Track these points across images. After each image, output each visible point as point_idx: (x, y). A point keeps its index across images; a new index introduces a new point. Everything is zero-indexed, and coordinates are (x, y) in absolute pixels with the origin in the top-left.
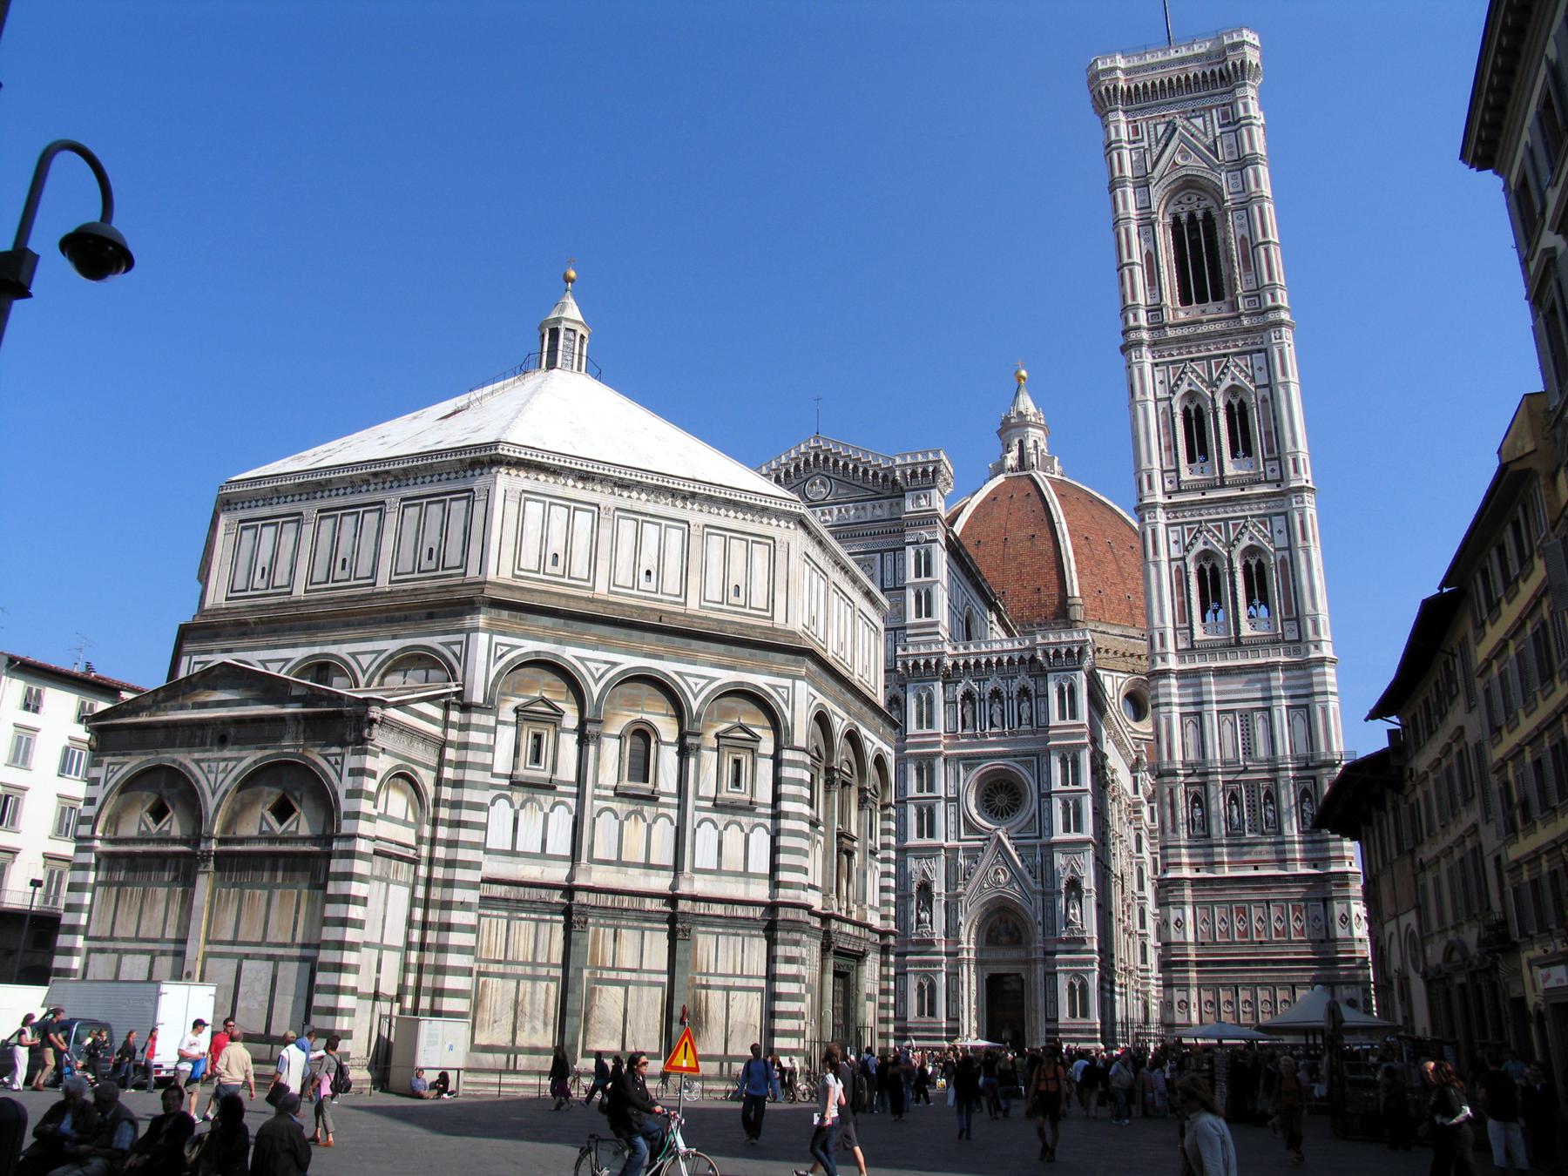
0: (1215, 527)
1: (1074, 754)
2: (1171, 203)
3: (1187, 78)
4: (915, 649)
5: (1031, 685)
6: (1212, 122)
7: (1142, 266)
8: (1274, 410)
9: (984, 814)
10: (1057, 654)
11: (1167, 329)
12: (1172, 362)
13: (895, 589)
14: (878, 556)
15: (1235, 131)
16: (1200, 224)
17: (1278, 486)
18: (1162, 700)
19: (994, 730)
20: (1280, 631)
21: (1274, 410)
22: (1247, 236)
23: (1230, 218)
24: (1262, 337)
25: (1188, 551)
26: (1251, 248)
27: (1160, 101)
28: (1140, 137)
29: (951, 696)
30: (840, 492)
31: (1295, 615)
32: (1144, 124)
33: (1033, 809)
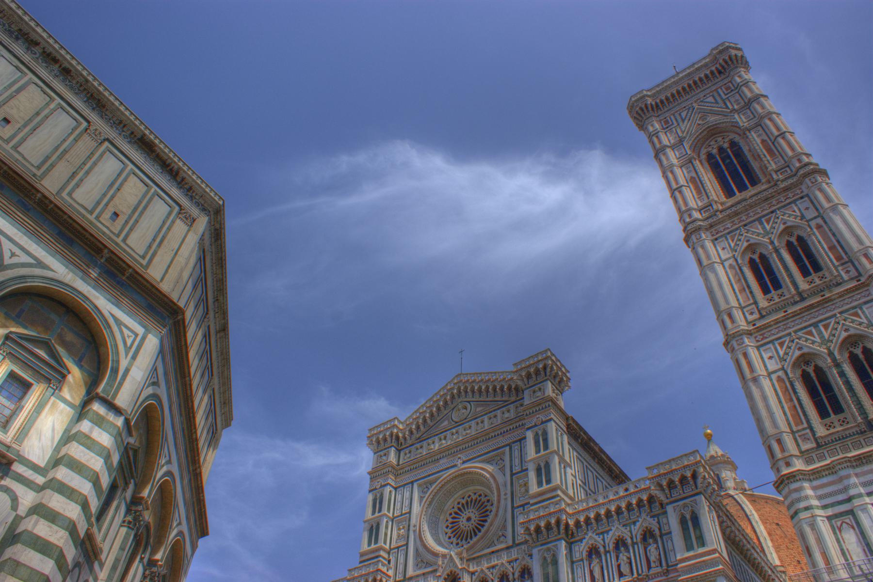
0: (806, 333)
2: (703, 147)
4: (536, 515)
5: (653, 524)
6: (719, 95)
7: (689, 187)
8: (831, 230)
10: (671, 483)
12: (729, 233)
13: (522, 471)
14: (507, 448)
15: (738, 92)
16: (729, 150)
17: (858, 281)
21: (831, 230)
22: (766, 138)
23: (748, 134)
24: (800, 189)
28: (671, 123)
29: (578, 555)
32: (672, 117)
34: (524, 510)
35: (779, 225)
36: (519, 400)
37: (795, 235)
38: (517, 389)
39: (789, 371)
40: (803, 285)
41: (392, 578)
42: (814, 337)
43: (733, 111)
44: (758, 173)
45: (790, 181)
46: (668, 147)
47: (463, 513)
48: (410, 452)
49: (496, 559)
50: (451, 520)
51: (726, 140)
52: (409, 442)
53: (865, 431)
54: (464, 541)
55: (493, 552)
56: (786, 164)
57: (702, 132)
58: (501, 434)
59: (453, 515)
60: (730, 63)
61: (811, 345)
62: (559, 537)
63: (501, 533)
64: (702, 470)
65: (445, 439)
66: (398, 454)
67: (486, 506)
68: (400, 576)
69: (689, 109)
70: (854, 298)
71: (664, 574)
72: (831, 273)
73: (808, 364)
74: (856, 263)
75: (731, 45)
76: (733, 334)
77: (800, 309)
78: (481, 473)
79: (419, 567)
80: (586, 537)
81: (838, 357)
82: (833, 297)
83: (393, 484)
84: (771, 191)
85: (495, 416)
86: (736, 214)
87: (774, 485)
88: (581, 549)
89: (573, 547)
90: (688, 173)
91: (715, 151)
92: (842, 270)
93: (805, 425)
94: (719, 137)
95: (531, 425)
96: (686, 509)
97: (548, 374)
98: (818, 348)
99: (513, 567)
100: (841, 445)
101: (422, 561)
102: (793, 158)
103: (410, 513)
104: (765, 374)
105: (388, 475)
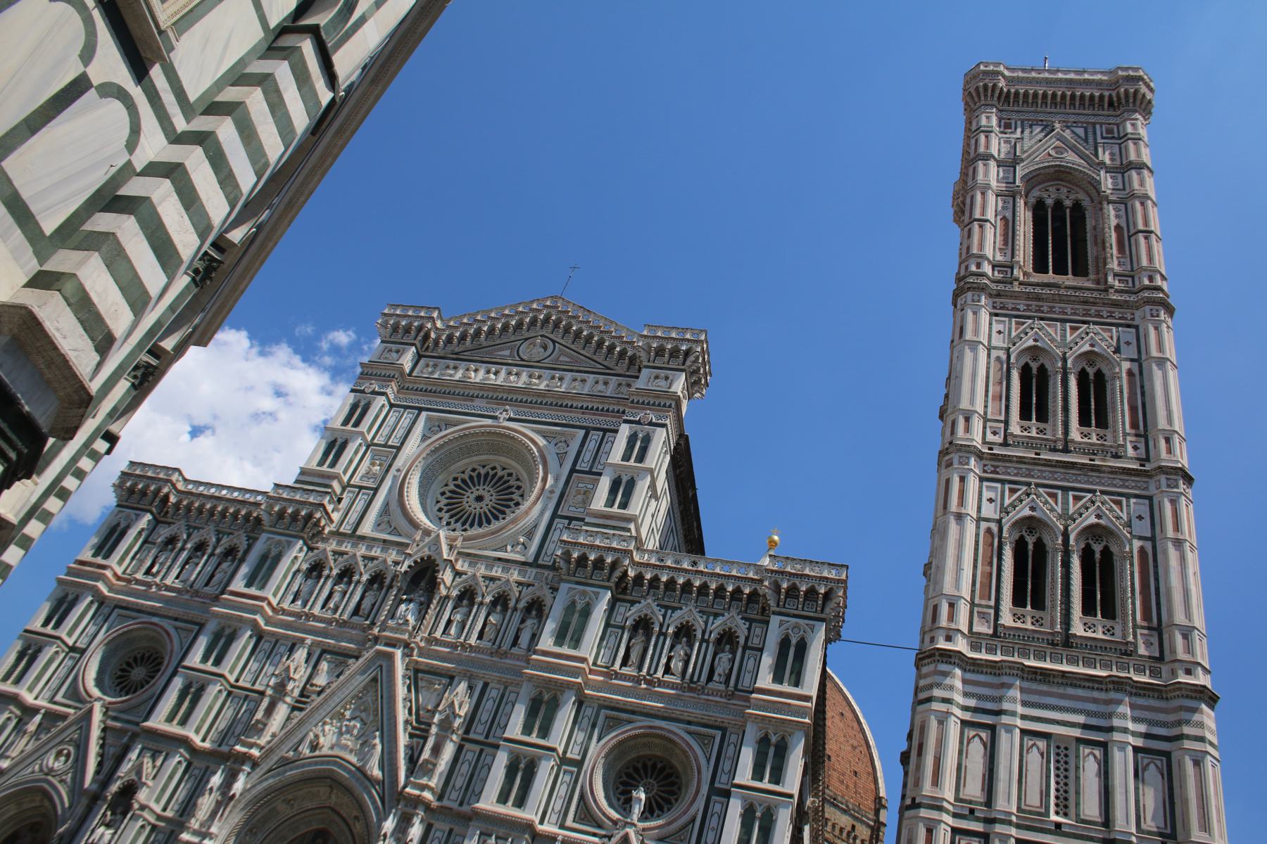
0: (1051, 495)
1: (783, 738)
2: (1038, 188)
3: (1073, 96)
5: (741, 629)
6: (1095, 133)
7: (995, 227)
8: (1142, 387)
9: (614, 801)
11: (1016, 283)
13: (590, 472)
14: (582, 432)
15: (1120, 144)
16: (1068, 211)
18: (937, 693)
19: (668, 678)
20: (1131, 638)
21: (1142, 387)
22: (1124, 225)
24: (1133, 314)
25: (1008, 513)
26: (1127, 235)
27: (1039, 109)
29: (619, 619)
30: (562, 358)
31: (1158, 627)
32: (1019, 123)
33: (692, 811)
34: (569, 524)
35: (1085, 343)
36: (628, 376)
37: (1096, 368)
38: (633, 360)
39: (1005, 529)
40: (1075, 435)
41: (334, 525)
42: (1056, 504)
43: (1102, 164)
44: (1090, 263)
45: (1125, 297)
46: (995, 159)
47: (475, 486)
48: (435, 366)
49: (500, 570)
50: (452, 487)
51: (1072, 197)
52: (440, 352)
53: (1057, 645)
54: (459, 524)
55: (500, 559)
56: (1132, 273)
57: (1049, 167)
58: (582, 408)
59: (459, 482)
60: (1131, 100)
61: (1048, 512)
62: (607, 584)
63: (522, 540)
64: (841, 593)
65: (496, 373)
66: (415, 360)
67: (513, 493)
68: (348, 527)
69: (1046, 126)
70: (1127, 484)
71: (726, 695)
72: (1115, 438)
73: (1031, 532)
74: (1151, 443)
75: (1145, 77)
76: (961, 445)
77: (1057, 461)
78: (529, 446)
79: (380, 528)
80: (642, 601)
81: (1072, 542)
82: (1104, 468)
83: (391, 397)
84: (1095, 294)
85: (583, 381)
86: (1038, 298)
87: (917, 654)
88: (630, 614)
89: (617, 605)
90: (1003, 208)
91: (1050, 202)
92: (1131, 442)
93: (992, 603)
94: (1064, 186)
95: (632, 418)
96: (796, 630)
97: (688, 363)
98: (1055, 519)
99: (520, 592)
100: (1021, 646)
101: (389, 522)
102: (1145, 270)
103: (399, 449)
104: (975, 517)
105: (391, 381)
